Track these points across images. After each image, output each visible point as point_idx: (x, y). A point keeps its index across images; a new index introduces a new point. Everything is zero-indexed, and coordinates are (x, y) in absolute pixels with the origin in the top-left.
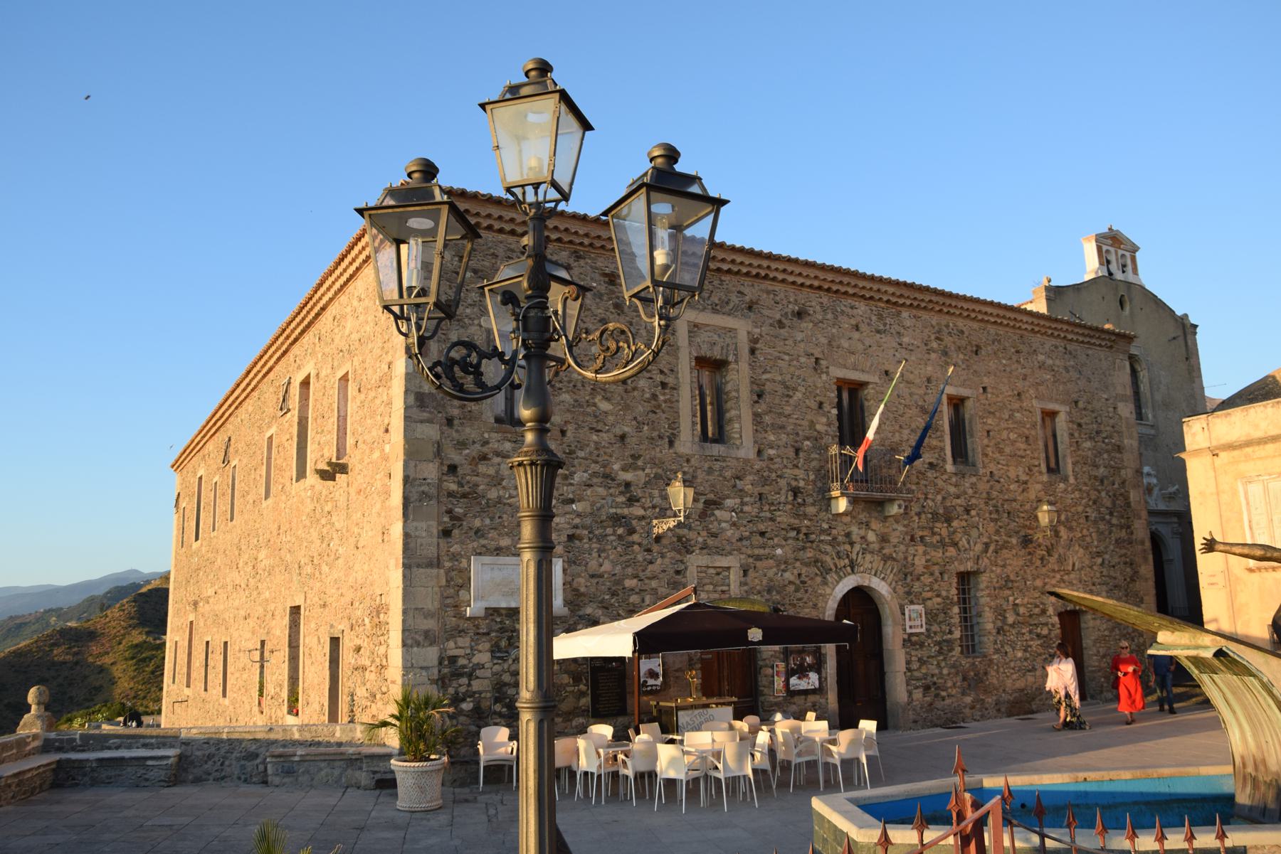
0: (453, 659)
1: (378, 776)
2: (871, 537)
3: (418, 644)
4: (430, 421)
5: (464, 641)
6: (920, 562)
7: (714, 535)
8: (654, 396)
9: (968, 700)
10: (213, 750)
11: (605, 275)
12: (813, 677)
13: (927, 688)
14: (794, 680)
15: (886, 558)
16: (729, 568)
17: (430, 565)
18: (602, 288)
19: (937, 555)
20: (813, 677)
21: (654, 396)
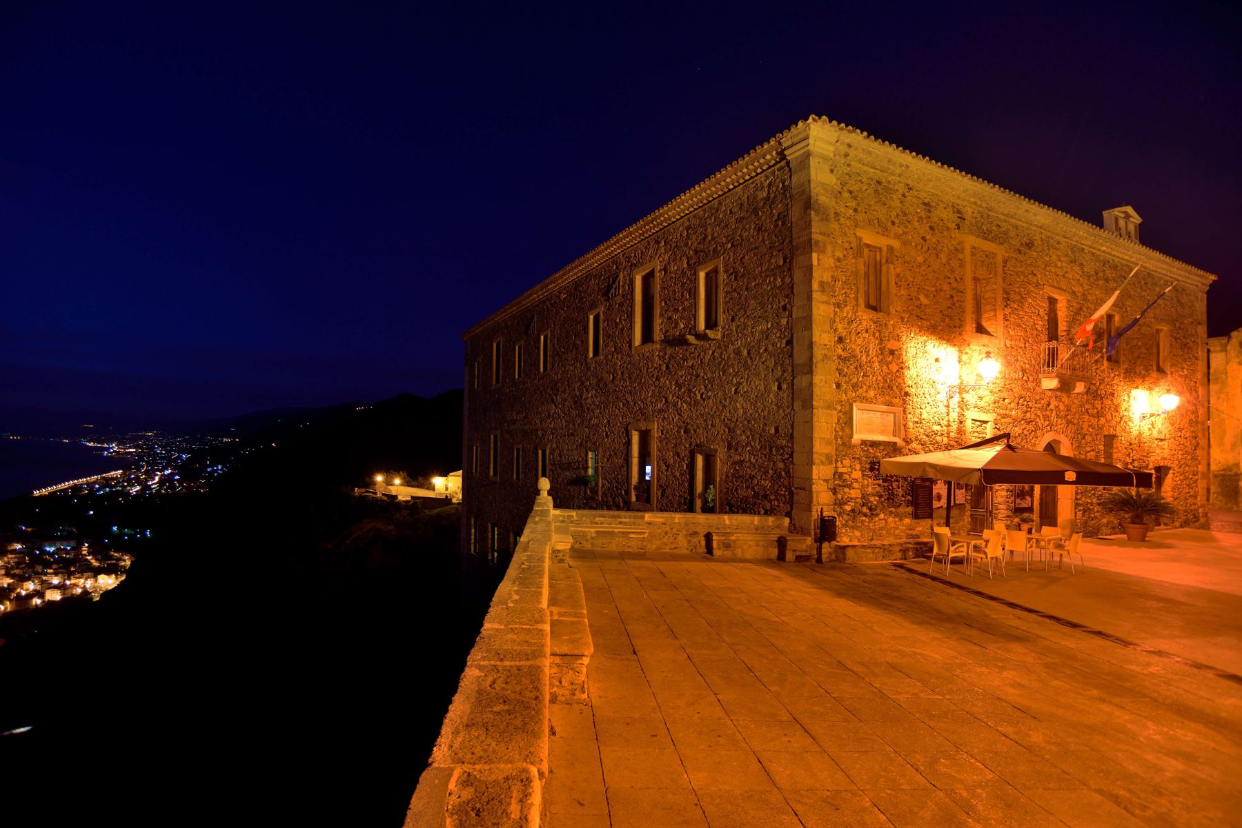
0: (841, 475)
1: (798, 553)
2: (1062, 407)
3: (823, 463)
4: (827, 303)
5: (847, 462)
6: (1086, 425)
7: (980, 398)
8: (952, 297)
9: (1105, 521)
10: (668, 528)
11: (925, 204)
12: (1028, 498)
13: (1084, 511)
14: (1018, 501)
15: (1069, 422)
16: (986, 422)
17: (829, 407)
18: (923, 214)
19: (1094, 421)
20: (1028, 498)
21: (952, 297)
